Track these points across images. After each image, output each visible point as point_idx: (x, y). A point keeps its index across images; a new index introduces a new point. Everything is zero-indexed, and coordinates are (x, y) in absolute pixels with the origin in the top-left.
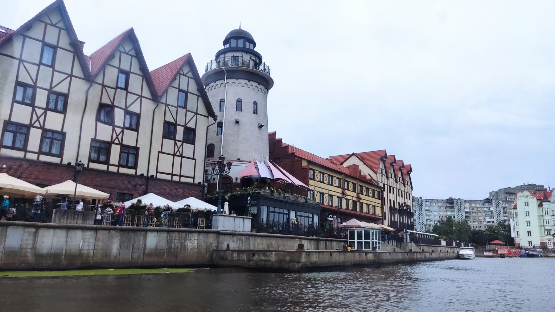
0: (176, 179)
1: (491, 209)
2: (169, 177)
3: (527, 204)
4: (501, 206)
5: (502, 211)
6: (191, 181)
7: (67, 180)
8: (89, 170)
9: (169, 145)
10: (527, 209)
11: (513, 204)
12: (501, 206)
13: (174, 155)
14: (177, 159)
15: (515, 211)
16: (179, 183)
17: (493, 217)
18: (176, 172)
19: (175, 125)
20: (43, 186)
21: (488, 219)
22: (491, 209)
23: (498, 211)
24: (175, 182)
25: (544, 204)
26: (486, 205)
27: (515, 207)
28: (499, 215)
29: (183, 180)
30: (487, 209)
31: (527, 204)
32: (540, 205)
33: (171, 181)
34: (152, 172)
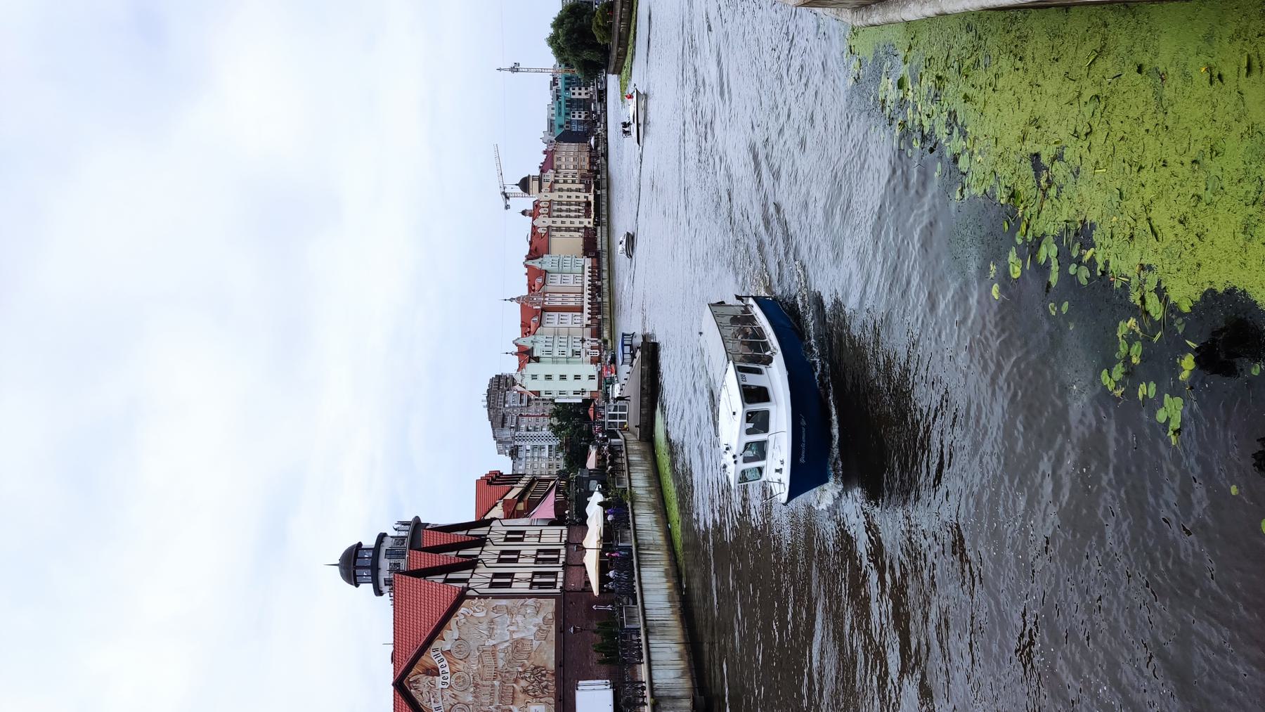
1: (529, 447)
3: (534, 377)
4: (524, 433)
5: (532, 433)
10: (541, 377)
11: (533, 397)
12: (524, 433)
15: (543, 395)
17: (542, 448)
21: (546, 454)
22: (529, 447)
23: (532, 438)
25: (535, 355)
26: (521, 454)
27: (537, 393)
28: (540, 438)
30: (529, 454)
31: (534, 377)
32: (537, 360)
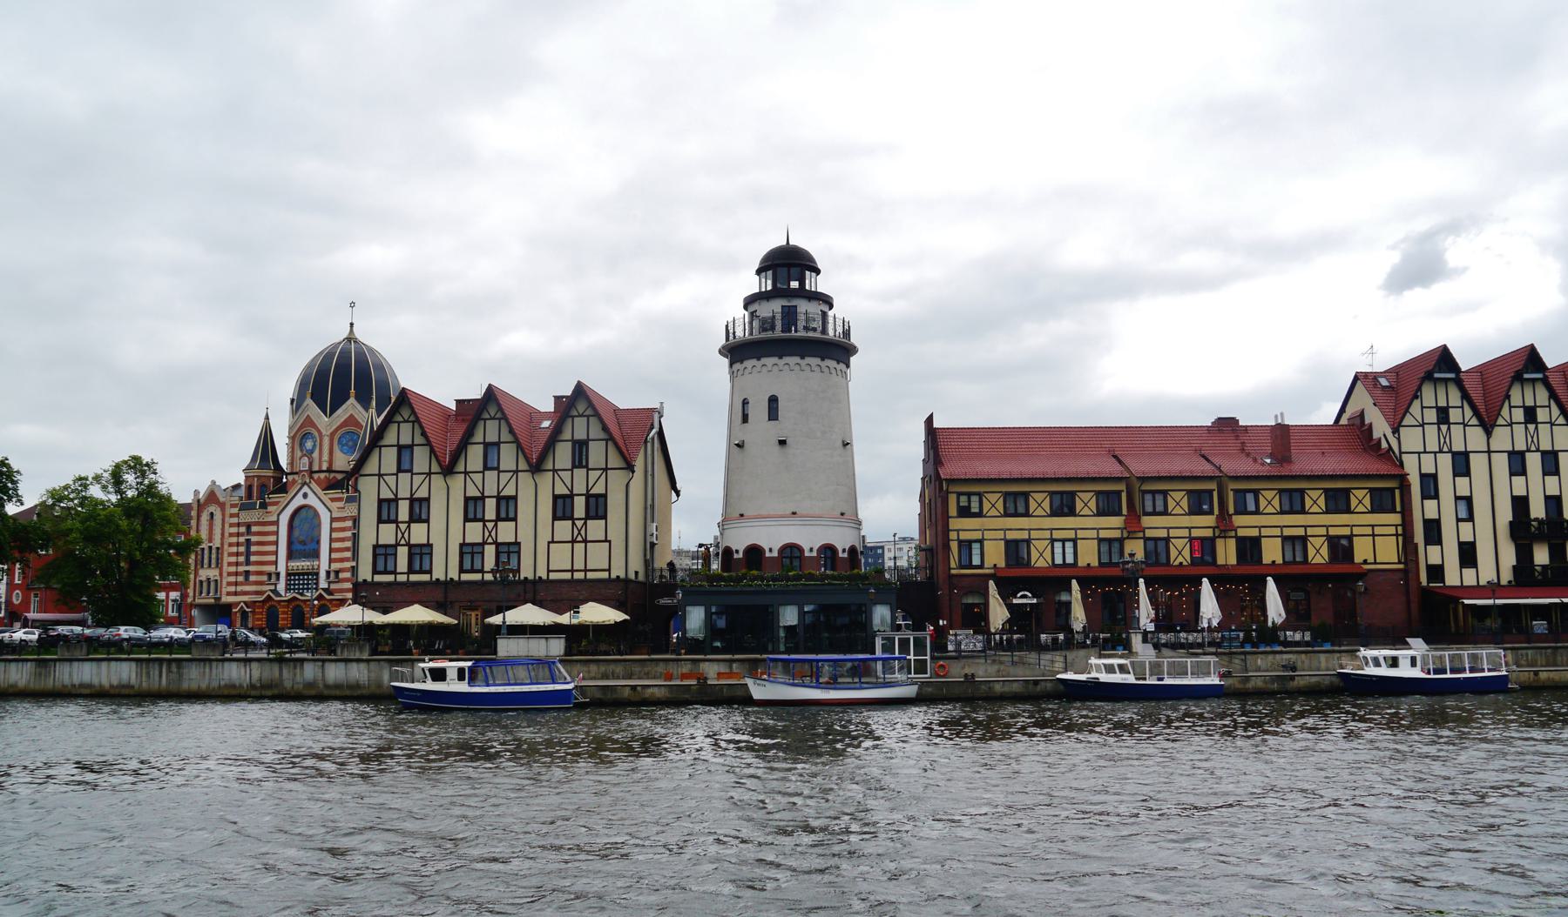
0: (579, 576)
2: (567, 576)
6: (605, 575)
7: (585, 601)
8: (460, 583)
9: (564, 529)
13: (573, 541)
14: (579, 547)
16: (586, 580)
18: (579, 565)
19: (571, 496)
20: (385, 612)
24: (579, 581)
29: (590, 575)
33: (572, 581)
34: (542, 573)
